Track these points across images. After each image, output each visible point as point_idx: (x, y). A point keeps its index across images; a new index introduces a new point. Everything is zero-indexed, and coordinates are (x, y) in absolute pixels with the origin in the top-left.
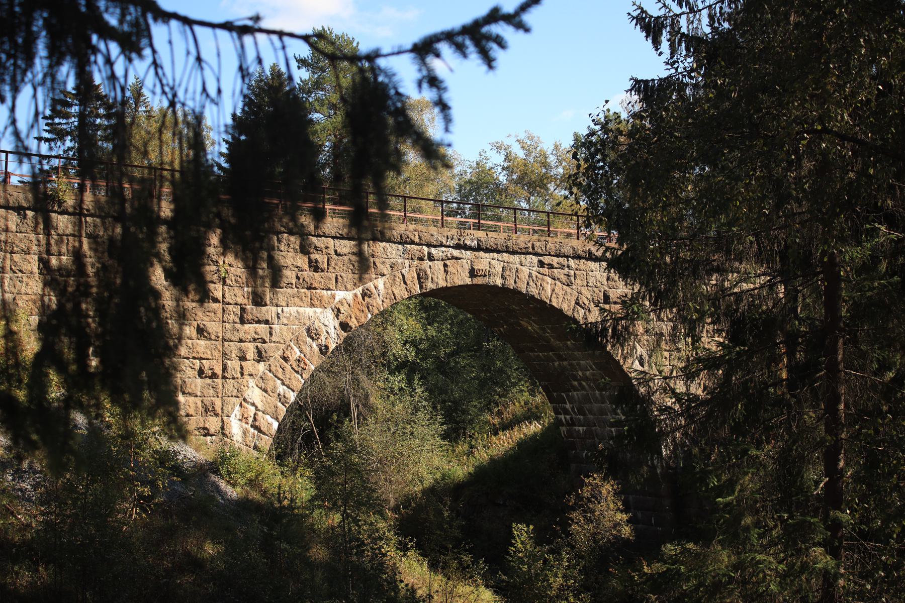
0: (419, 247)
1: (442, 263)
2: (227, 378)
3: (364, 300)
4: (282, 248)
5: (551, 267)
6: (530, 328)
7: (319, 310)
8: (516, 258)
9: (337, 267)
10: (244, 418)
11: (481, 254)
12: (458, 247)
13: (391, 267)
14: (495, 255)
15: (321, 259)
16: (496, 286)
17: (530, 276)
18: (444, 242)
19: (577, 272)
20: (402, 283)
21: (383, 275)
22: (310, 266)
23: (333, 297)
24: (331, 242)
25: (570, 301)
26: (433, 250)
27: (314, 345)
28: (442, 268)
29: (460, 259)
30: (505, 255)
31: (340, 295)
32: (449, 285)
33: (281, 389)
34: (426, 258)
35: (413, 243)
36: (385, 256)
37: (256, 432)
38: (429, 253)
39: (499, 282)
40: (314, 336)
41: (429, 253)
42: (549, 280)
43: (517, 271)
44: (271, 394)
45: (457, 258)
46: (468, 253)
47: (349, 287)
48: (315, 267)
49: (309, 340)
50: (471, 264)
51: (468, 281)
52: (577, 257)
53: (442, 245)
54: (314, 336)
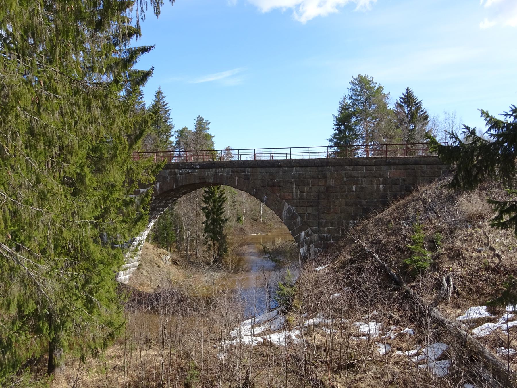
0: (174, 170)
12: (190, 168)
17: (227, 177)
21: (159, 182)
23: (140, 191)
30: (214, 170)
32: (188, 183)
35: (171, 169)
39: (211, 181)
42: (237, 178)
45: (191, 173)
51: (198, 181)
52: (251, 167)
53: (183, 169)
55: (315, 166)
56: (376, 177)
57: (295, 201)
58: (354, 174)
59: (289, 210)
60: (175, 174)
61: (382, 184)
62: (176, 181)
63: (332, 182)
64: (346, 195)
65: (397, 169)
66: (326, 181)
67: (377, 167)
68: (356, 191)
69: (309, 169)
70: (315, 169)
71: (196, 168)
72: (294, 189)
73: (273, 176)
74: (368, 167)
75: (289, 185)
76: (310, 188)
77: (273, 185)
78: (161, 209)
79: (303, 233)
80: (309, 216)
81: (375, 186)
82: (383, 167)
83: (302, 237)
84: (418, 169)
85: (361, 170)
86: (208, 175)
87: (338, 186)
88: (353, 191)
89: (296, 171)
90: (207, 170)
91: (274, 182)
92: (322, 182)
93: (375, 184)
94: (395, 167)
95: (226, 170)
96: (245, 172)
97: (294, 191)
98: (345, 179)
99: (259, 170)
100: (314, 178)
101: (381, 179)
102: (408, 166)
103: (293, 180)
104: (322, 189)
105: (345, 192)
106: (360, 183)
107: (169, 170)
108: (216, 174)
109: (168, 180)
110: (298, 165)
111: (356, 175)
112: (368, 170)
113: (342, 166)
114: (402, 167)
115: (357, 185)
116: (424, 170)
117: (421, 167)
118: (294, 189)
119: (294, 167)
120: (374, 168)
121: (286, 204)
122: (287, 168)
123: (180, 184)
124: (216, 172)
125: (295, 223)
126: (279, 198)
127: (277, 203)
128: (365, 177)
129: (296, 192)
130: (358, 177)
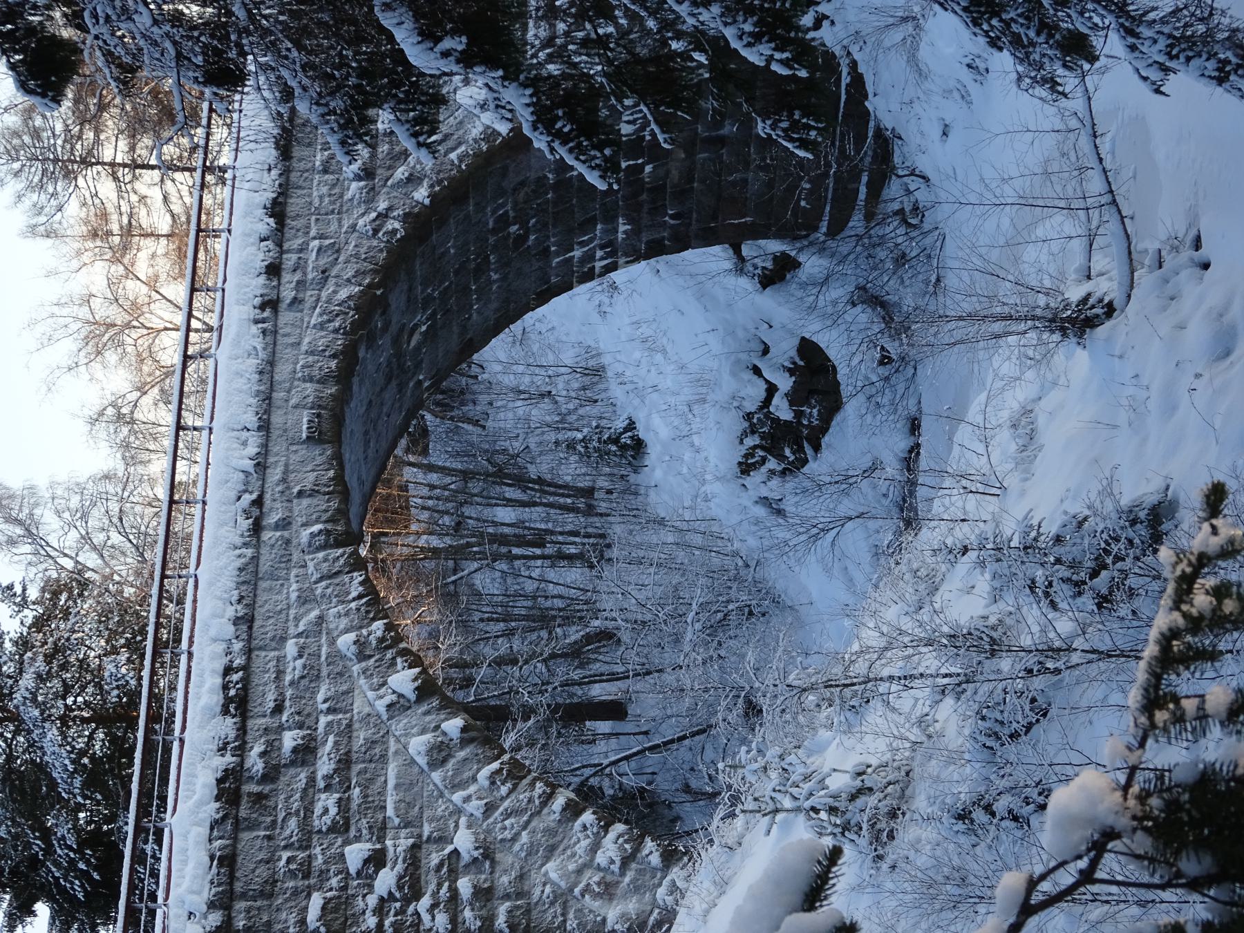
0: (264, 551)
1: (295, 501)
2: (528, 925)
3: (370, 657)
4: (269, 819)
5: (301, 284)
6: (424, 328)
8: (286, 353)
9: (306, 712)
13: (304, 604)
14: (278, 395)
15: (289, 740)
18: (254, 496)
19: (313, 233)
20: (336, 581)
22: (304, 763)
24: (256, 724)
26: (273, 518)
27: (462, 754)
28: (305, 502)
29: (286, 465)
34: (286, 534)
36: (283, 616)
37: (634, 865)
38: (277, 527)
40: (444, 754)
41: (277, 527)
43: (312, 353)
44: (558, 838)
45: (286, 472)
47: (344, 688)
48: (306, 753)
50: (298, 443)
54: (444, 754)
127: (450, 143)
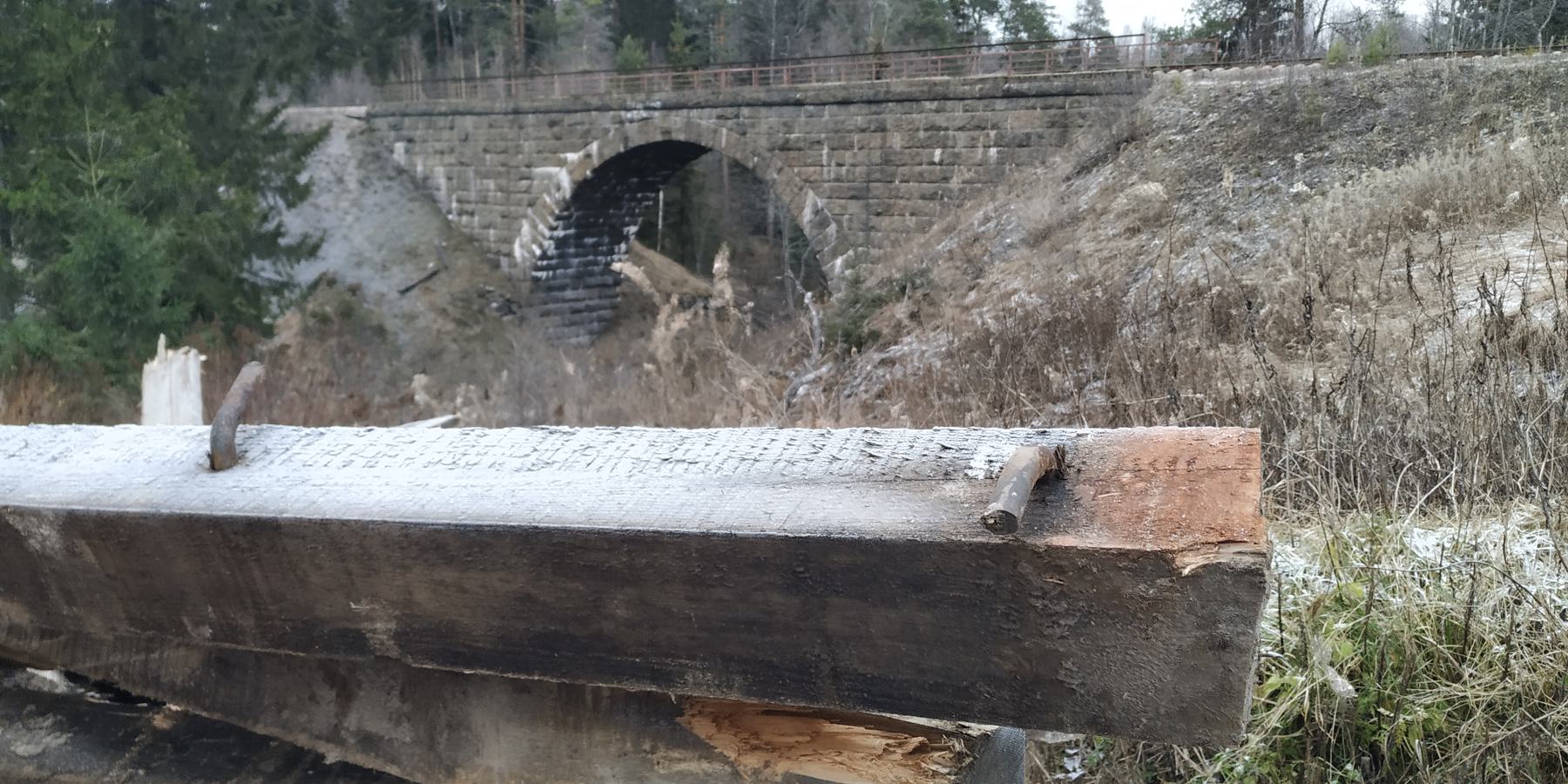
7: (557, 169)
8: (694, 113)
10: (522, 246)
11: (665, 112)
12: (647, 108)
16: (680, 143)
21: (596, 139)
25: (744, 150)
26: (629, 115)
30: (685, 112)
31: (572, 157)
33: (541, 227)
39: (682, 137)
42: (724, 131)
46: (656, 114)
49: (553, 191)
51: (659, 138)
52: (748, 105)
55: (863, 102)
56: (984, 129)
57: (826, 185)
58: (940, 120)
59: (815, 205)
60: (622, 122)
61: (995, 146)
62: (626, 139)
63: (896, 141)
64: (921, 174)
65: (1027, 108)
66: (884, 139)
67: (986, 102)
68: (941, 163)
69: (852, 108)
70: (865, 109)
71: (655, 109)
72: (825, 157)
73: (789, 127)
74: (967, 102)
75: (817, 147)
76: (855, 154)
77: (785, 147)
78: (639, 195)
79: (839, 261)
80: (850, 220)
81: (980, 150)
82: (998, 102)
83: (837, 270)
84: (1071, 107)
85: (953, 111)
86: (675, 122)
87: (907, 151)
88: (934, 163)
89: (831, 116)
90: (674, 113)
91: (787, 141)
92: (876, 140)
93: (980, 145)
94: (1023, 102)
95: (707, 111)
96: (737, 116)
97: (825, 163)
98: (922, 134)
99: (763, 111)
100: (863, 131)
101: (993, 133)
102: (1050, 101)
103: (823, 136)
104: (876, 156)
105: (921, 164)
106: (950, 143)
107: (612, 113)
108: (689, 125)
109: (611, 134)
110: (831, 100)
111: (944, 125)
112: (967, 111)
113: (917, 100)
114: (1039, 102)
115: (944, 147)
116: (1086, 109)
117: (1079, 102)
118: (825, 157)
119: (824, 104)
120: (981, 104)
121: (811, 193)
122: (811, 108)
123: (631, 145)
124: (689, 118)
125: (825, 237)
126: (797, 179)
128: (960, 129)
129: (829, 165)
130: (946, 129)
